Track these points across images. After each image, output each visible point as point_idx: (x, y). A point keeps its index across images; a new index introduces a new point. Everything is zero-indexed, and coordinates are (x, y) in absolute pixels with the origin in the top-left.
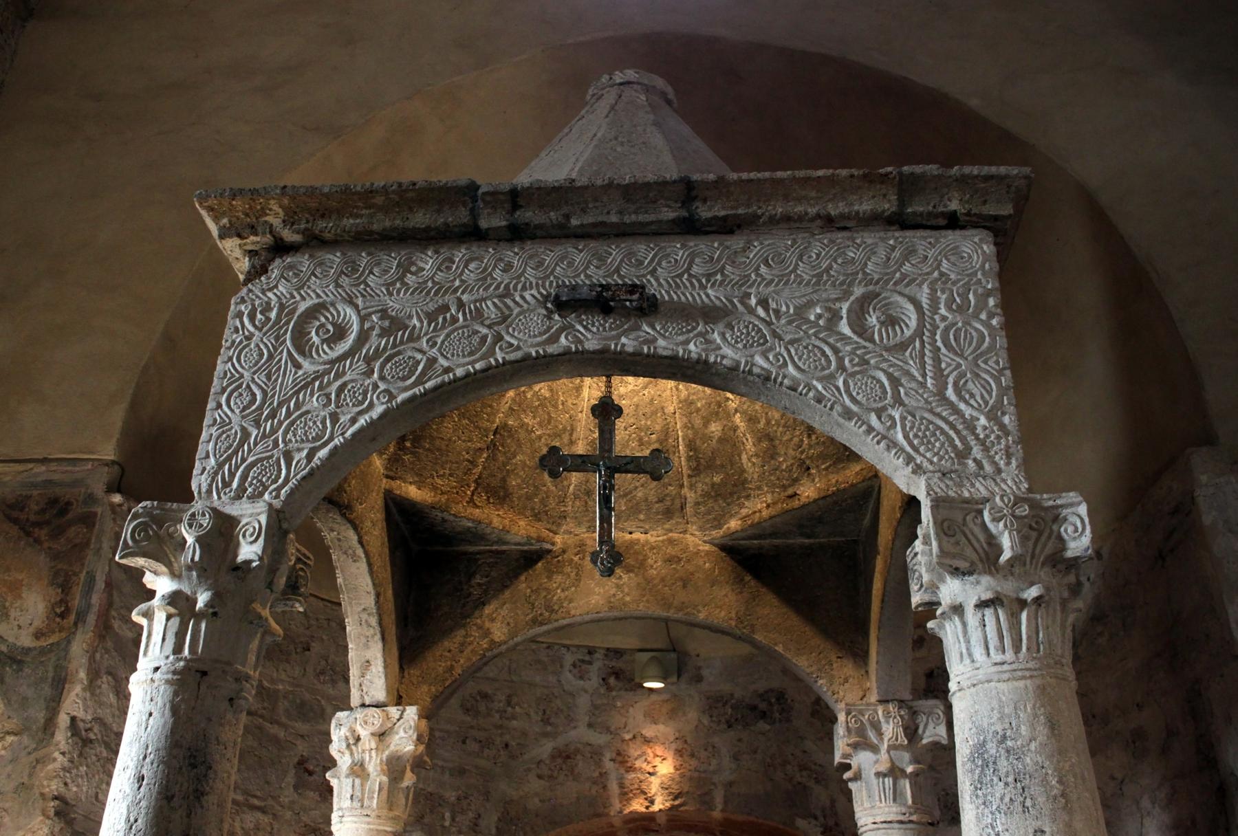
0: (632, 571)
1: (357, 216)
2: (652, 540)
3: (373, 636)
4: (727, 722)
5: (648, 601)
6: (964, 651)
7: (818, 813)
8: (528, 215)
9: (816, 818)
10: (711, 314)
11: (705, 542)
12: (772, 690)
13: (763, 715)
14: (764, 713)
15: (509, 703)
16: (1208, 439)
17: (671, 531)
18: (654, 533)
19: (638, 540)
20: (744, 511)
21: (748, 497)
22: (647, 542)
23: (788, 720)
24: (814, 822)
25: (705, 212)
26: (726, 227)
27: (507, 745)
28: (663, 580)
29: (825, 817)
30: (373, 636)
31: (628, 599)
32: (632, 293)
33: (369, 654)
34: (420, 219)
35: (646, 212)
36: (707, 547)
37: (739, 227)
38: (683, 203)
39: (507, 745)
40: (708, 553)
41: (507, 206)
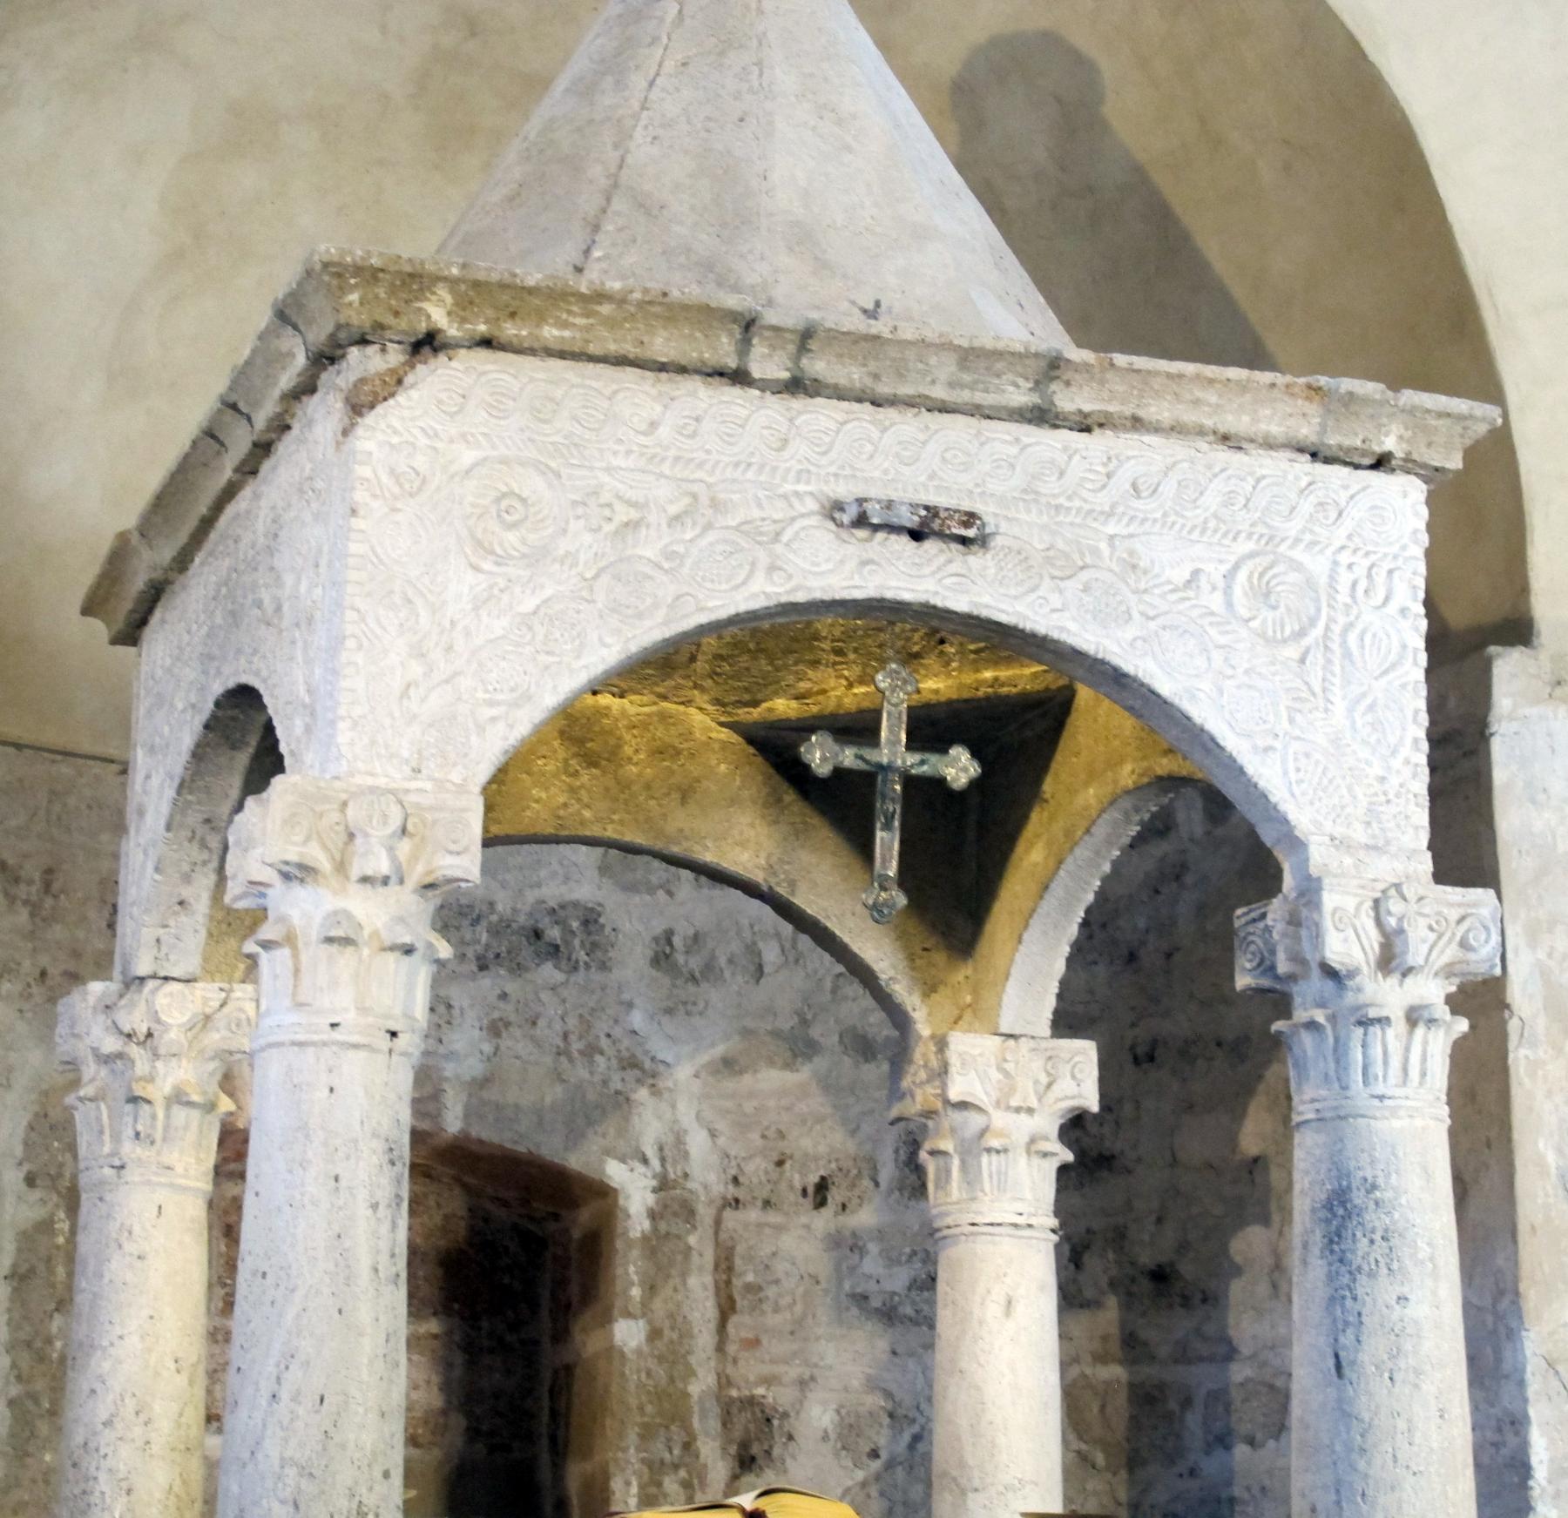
0: (595, 765)
1: (565, 325)
2: (632, 710)
3: (205, 863)
4: (478, 958)
5: (621, 822)
6: (1332, 1073)
7: (651, 1153)
8: (818, 366)
9: (645, 1161)
10: (1064, 565)
11: (722, 724)
12: (576, 904)
13: (554, 951)
14: (557, 947)
15: (47, 886)
16: (1518, 631)
17: (664, 698)
18: (633, 697)
19: (608, 708)
20: (803, 686)
21: (815, 663)
22: (623, 712)
23: (604, 966)
24: (640, 1168)
25: (1068, 400)
26: (1084, 426)
27: (43, 974)
28: (648, 787)
29: (663, 1160)
30: (205, 863)
31: (587, 814)
32: (967, 525)
33: (186, 892)
34: (662, 346)
35: (986, 391)
36: (725, 734)
37: (1101, 425)
38: (1037, 383)
39: (43, 974)
40: (725, 745)
41: (792, 348)
